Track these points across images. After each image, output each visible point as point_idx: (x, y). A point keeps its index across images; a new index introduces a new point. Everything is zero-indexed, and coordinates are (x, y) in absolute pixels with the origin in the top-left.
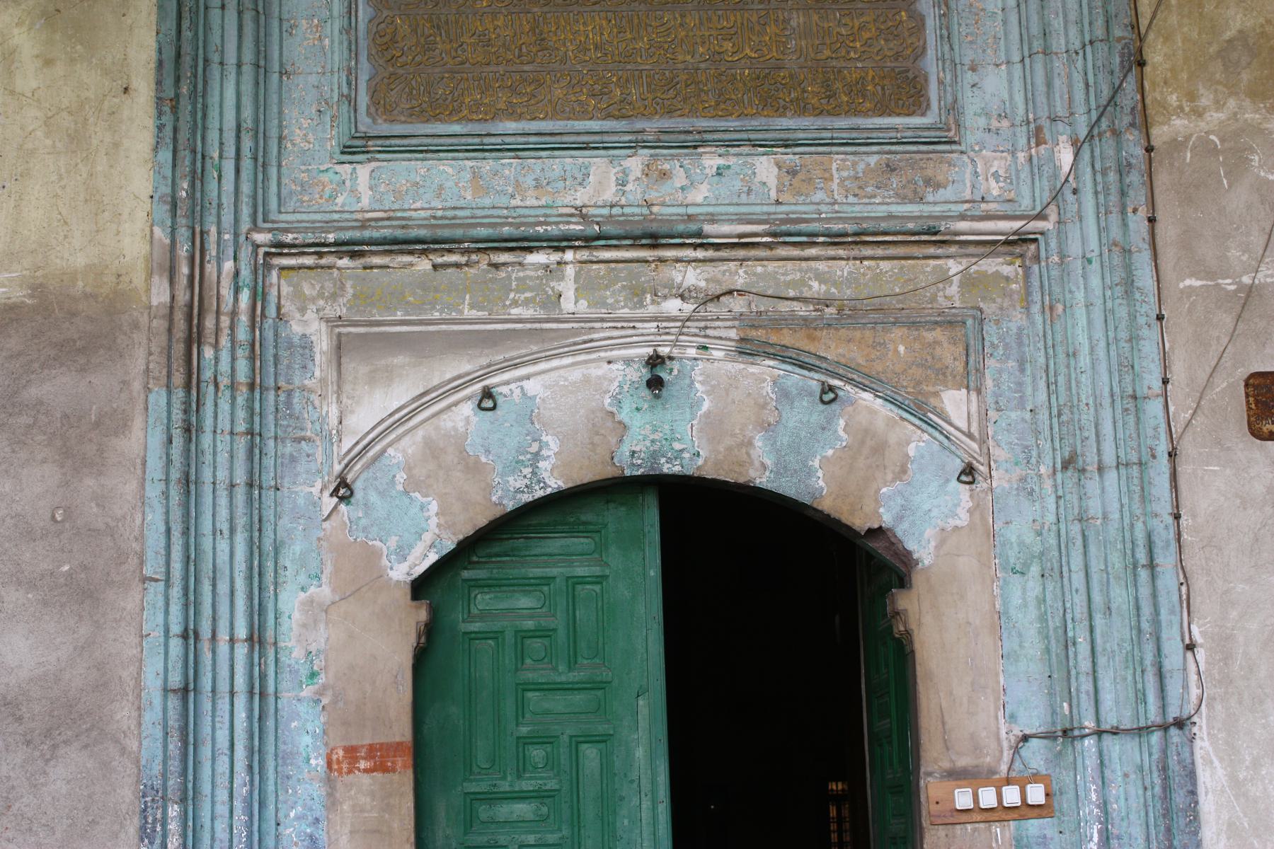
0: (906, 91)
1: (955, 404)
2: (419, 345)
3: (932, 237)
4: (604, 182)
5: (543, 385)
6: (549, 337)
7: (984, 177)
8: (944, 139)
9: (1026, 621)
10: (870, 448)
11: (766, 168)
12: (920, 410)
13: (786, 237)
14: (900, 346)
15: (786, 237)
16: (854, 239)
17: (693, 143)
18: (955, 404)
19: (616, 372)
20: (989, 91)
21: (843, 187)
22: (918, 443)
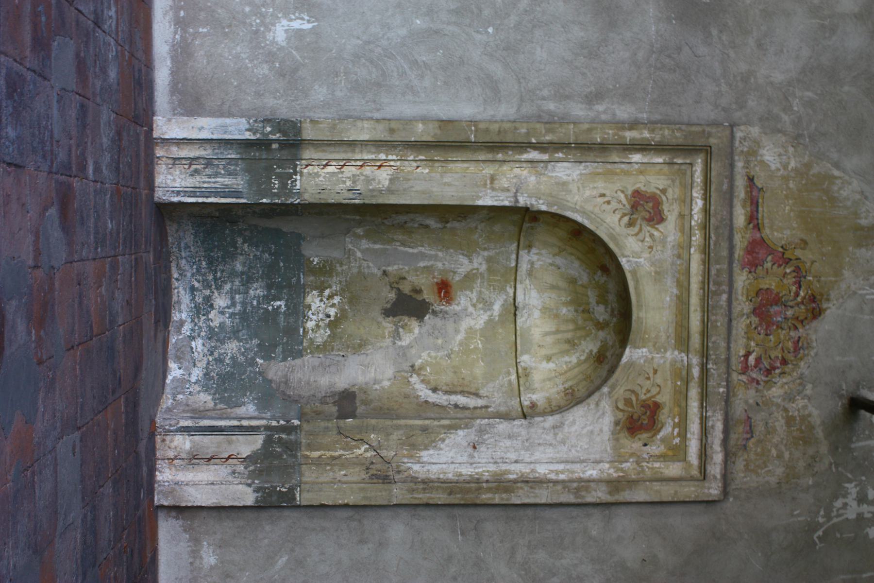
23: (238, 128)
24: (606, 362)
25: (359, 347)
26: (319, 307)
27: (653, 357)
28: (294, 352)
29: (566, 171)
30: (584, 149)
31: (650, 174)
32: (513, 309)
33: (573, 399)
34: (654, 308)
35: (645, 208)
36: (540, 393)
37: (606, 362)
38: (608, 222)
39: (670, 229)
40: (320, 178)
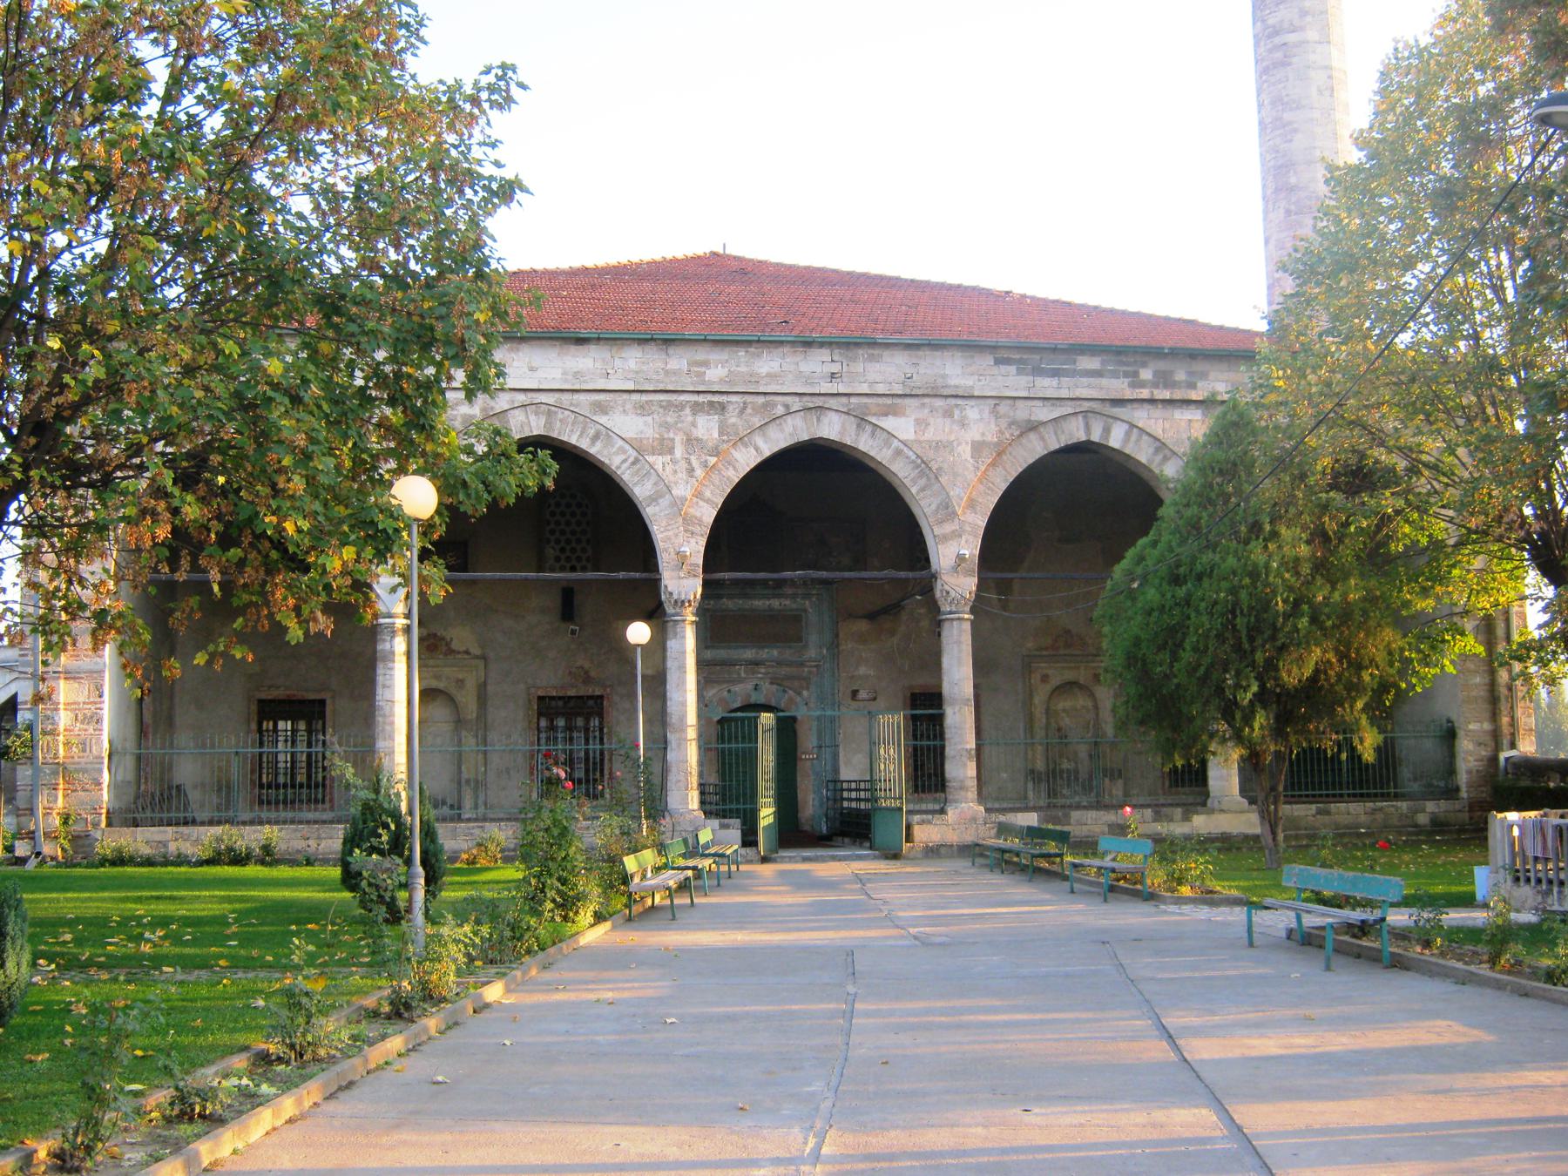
0: (799, 639)
1: (805, 693)
2: (718, 682)
3: (802, 664)
4: (749, 654)
5: (737, 688)
6: (740, 681)
7: (812, 653)
8: (806, 646)
9: (814, 728)
10: (791, 700)
11: (775, 653)
12: (799, 694)
13: (779, 663)
14: (796, 683)
15: (779, 663)
16: (789, 664)
17: (763, 648)
18: (805, 693)
19: (750, 686)
20: (813, 638)
21: (788, 654)
22: (798, 699)
23: (1030, 785)
24: (1081, 687)
25: (1076, 753)
26: (1065, 765)
27: (1082, 676)
28: (1077, 772)
29: (1036, 700)
30: (1031, 696)
31: (1036, 678)
32: (1064, 710)
33: (1092, 695)
34: (1069, 676)
35: (1045, 679)
36: (1089, 704)
37: (1081, 687)
38: (1048, 688)
39: (1050, 672)
40: (1040, 765)
